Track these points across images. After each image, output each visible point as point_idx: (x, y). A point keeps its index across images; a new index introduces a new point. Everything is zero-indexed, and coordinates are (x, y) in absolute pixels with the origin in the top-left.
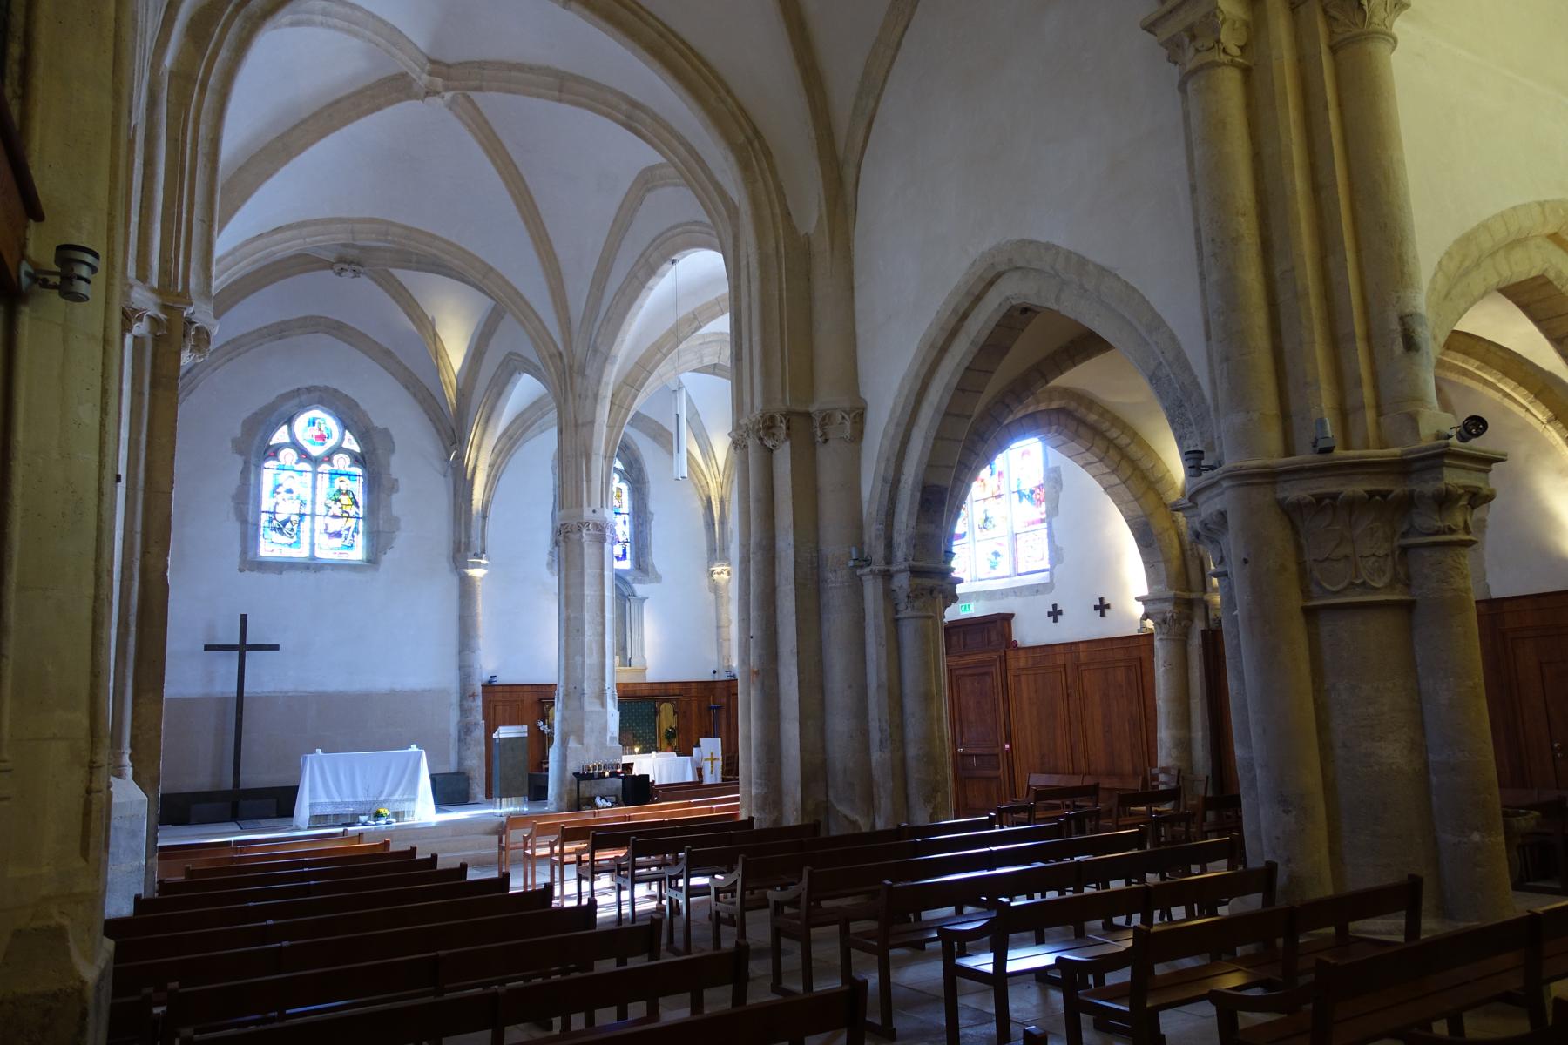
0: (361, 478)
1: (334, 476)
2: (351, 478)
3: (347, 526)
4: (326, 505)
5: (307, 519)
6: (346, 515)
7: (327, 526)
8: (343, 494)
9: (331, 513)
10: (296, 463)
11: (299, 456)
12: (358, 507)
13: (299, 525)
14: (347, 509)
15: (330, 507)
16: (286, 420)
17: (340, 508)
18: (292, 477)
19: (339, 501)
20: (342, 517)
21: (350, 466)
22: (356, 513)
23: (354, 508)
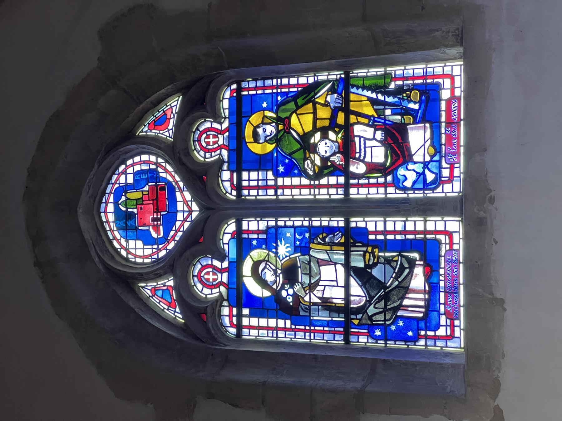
0: (244, 85)
1: (244, 157)
2: (245, 108)
3: (369, 110)
4: (318, 176)
5: (358, 222)
6: (341, 118)
7: (373, 168)
8: (288, 128)
9: (337, 159)
10: (222, 257)
11: (205, 253)
12: (318, 85)
13: (376, 244)
14: (324, 113)
15: (325, 160)
16: (120, 291)
17: (325, 136)
18: (256, 265)
19: (305, 137)
20: (347, 128)
21: (217, 118)
22: (332, 91)
23: (322, 96)
